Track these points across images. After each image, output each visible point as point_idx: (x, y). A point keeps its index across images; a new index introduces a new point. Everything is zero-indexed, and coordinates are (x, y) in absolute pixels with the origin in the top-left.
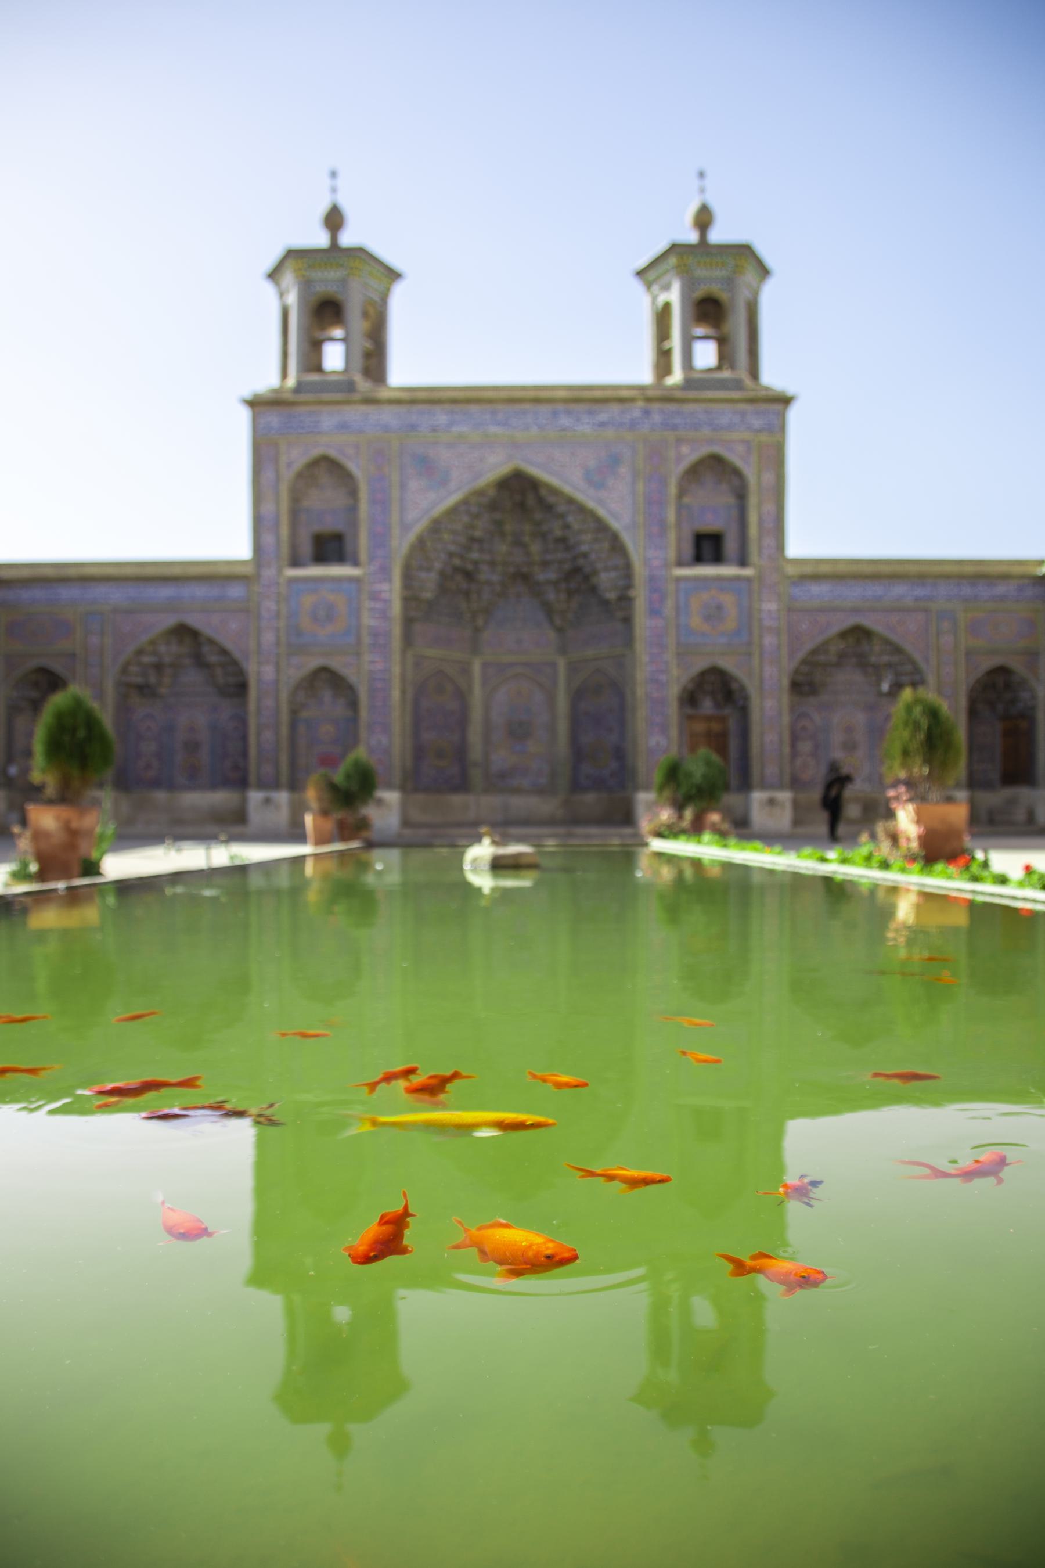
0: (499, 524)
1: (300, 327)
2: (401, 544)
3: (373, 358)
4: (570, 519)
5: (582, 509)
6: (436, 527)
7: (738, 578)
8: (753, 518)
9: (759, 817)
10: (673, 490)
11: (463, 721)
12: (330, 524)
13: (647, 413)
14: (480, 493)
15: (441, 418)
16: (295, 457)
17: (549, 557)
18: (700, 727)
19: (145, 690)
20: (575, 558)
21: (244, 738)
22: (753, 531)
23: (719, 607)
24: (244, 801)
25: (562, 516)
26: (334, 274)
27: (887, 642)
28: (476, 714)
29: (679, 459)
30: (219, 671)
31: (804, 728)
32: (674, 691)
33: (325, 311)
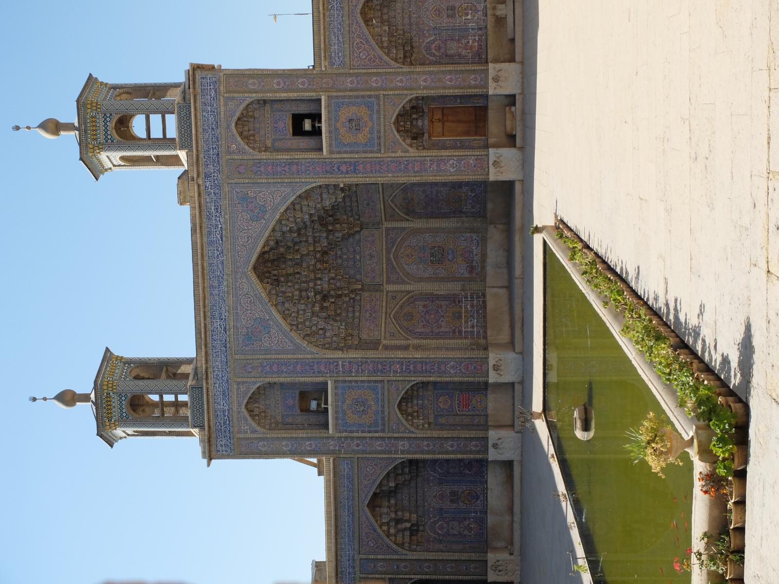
1: (154, 427)
2: (311, 352)
5: (280, 221)
6: (295, 326)
7: (328, 106)
8: (284, 95)
9: (509, 87)
10: (264, 156)
11: (432, 298)
12: (294, 400)
13: (207, 176)
14: (269, 294)
15: (218, 323)
16: (247, 427)
17: (311, 240)
18: (438, 127)
19: (414, 530)
20: (313, 221)
21: (447, 461)
22: (293, 95)
23: (350, 121)
24: (493, 462)
26: (115, 402)
29: (240, 151)
30: (401, 479)
31: (439, 48)
32: (413, 152)
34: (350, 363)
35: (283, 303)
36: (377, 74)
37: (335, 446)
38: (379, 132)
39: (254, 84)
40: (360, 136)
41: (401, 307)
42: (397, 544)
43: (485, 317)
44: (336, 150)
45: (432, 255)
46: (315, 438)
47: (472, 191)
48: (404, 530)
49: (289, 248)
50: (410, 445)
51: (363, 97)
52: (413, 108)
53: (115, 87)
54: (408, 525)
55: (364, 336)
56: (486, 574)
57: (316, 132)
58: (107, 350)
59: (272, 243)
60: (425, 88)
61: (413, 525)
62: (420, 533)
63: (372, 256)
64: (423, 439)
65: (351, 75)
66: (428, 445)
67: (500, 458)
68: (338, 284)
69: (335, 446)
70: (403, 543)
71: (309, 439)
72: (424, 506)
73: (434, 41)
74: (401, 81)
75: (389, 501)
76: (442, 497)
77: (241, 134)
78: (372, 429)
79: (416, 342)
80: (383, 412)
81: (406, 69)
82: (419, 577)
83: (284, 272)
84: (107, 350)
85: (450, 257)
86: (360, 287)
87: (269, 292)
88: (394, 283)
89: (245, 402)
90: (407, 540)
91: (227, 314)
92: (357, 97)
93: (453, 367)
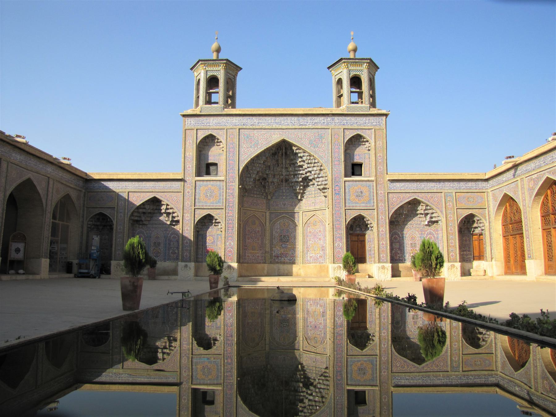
0: (277, 161)
3: (230, 99)
4: (304, 158)
20: (306, 173)
24: (177, 265)
25: (301, 157)
27: (427, 206)
28: (268, 234)
31: (396, 238)
33: (212, 82)
34: (233, 189)
35: (265, 156)
36: (385, 206)
37: (189, 180)
38: (356, 206)
39: (379, 144)
40: (354, 197)
41: (258, 219)
42: (132, 213)
43: (253, 263)
44: (347, 183)
45: (284, 236)
46: (192, 170)
47: (321, 257)
48: (140, 217)
49: (292, 160)
50: (188, 220)
51: (374, 199)
52: (367, 225)
53: (374, 78)
54: (143, 219)
55: (245, 199)
56: (115, 260)
57: (353, 174)
58: (241, 69)
59: (297, 151)
60: (378, 231)
61: (142, 221)
62: (137, 225)
63: (284, 205)
64: (190, 227)
65: (384, 193)
66: (187, 230)
67: (179, 268)
68: (271, 187)
69: (189, 180)
70: (133, 216)
71: (192, 167)
72: (153, 228)
73: (399, 236)
74: (382, 219)
75: (156, 209)
76: (157, 238)
77: (353, 137)
78: (197, 200)
79: (242, 227)
80: (206, 206)
81: (387, 221)
82: (115, 223)
83: (280, 158)
84: (241, 69)
85: (283, 246)
86: (269, 197)
87: (272, 149)
88: (270, 216)
89: (214, 134)
90: (136, 218)
91: (261, 126)
92: (373, 196)
93: (230, 244)
